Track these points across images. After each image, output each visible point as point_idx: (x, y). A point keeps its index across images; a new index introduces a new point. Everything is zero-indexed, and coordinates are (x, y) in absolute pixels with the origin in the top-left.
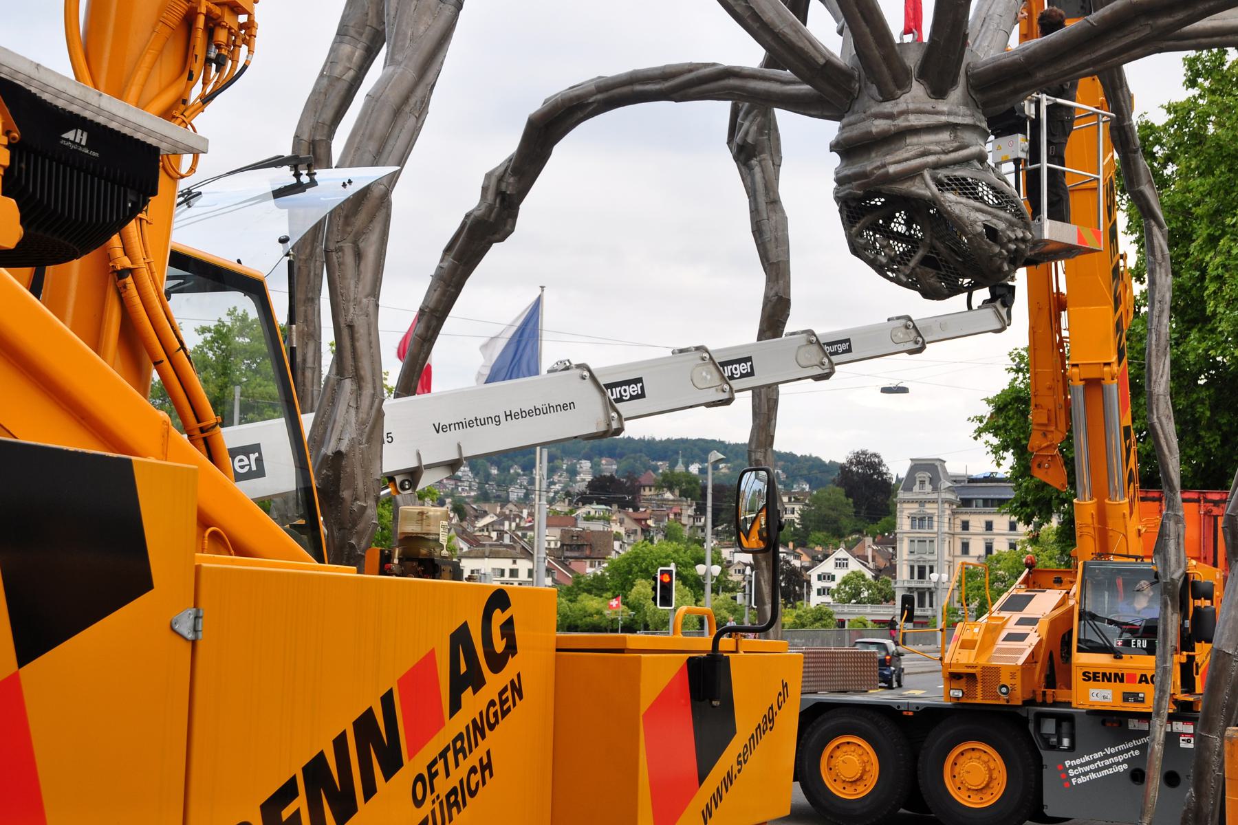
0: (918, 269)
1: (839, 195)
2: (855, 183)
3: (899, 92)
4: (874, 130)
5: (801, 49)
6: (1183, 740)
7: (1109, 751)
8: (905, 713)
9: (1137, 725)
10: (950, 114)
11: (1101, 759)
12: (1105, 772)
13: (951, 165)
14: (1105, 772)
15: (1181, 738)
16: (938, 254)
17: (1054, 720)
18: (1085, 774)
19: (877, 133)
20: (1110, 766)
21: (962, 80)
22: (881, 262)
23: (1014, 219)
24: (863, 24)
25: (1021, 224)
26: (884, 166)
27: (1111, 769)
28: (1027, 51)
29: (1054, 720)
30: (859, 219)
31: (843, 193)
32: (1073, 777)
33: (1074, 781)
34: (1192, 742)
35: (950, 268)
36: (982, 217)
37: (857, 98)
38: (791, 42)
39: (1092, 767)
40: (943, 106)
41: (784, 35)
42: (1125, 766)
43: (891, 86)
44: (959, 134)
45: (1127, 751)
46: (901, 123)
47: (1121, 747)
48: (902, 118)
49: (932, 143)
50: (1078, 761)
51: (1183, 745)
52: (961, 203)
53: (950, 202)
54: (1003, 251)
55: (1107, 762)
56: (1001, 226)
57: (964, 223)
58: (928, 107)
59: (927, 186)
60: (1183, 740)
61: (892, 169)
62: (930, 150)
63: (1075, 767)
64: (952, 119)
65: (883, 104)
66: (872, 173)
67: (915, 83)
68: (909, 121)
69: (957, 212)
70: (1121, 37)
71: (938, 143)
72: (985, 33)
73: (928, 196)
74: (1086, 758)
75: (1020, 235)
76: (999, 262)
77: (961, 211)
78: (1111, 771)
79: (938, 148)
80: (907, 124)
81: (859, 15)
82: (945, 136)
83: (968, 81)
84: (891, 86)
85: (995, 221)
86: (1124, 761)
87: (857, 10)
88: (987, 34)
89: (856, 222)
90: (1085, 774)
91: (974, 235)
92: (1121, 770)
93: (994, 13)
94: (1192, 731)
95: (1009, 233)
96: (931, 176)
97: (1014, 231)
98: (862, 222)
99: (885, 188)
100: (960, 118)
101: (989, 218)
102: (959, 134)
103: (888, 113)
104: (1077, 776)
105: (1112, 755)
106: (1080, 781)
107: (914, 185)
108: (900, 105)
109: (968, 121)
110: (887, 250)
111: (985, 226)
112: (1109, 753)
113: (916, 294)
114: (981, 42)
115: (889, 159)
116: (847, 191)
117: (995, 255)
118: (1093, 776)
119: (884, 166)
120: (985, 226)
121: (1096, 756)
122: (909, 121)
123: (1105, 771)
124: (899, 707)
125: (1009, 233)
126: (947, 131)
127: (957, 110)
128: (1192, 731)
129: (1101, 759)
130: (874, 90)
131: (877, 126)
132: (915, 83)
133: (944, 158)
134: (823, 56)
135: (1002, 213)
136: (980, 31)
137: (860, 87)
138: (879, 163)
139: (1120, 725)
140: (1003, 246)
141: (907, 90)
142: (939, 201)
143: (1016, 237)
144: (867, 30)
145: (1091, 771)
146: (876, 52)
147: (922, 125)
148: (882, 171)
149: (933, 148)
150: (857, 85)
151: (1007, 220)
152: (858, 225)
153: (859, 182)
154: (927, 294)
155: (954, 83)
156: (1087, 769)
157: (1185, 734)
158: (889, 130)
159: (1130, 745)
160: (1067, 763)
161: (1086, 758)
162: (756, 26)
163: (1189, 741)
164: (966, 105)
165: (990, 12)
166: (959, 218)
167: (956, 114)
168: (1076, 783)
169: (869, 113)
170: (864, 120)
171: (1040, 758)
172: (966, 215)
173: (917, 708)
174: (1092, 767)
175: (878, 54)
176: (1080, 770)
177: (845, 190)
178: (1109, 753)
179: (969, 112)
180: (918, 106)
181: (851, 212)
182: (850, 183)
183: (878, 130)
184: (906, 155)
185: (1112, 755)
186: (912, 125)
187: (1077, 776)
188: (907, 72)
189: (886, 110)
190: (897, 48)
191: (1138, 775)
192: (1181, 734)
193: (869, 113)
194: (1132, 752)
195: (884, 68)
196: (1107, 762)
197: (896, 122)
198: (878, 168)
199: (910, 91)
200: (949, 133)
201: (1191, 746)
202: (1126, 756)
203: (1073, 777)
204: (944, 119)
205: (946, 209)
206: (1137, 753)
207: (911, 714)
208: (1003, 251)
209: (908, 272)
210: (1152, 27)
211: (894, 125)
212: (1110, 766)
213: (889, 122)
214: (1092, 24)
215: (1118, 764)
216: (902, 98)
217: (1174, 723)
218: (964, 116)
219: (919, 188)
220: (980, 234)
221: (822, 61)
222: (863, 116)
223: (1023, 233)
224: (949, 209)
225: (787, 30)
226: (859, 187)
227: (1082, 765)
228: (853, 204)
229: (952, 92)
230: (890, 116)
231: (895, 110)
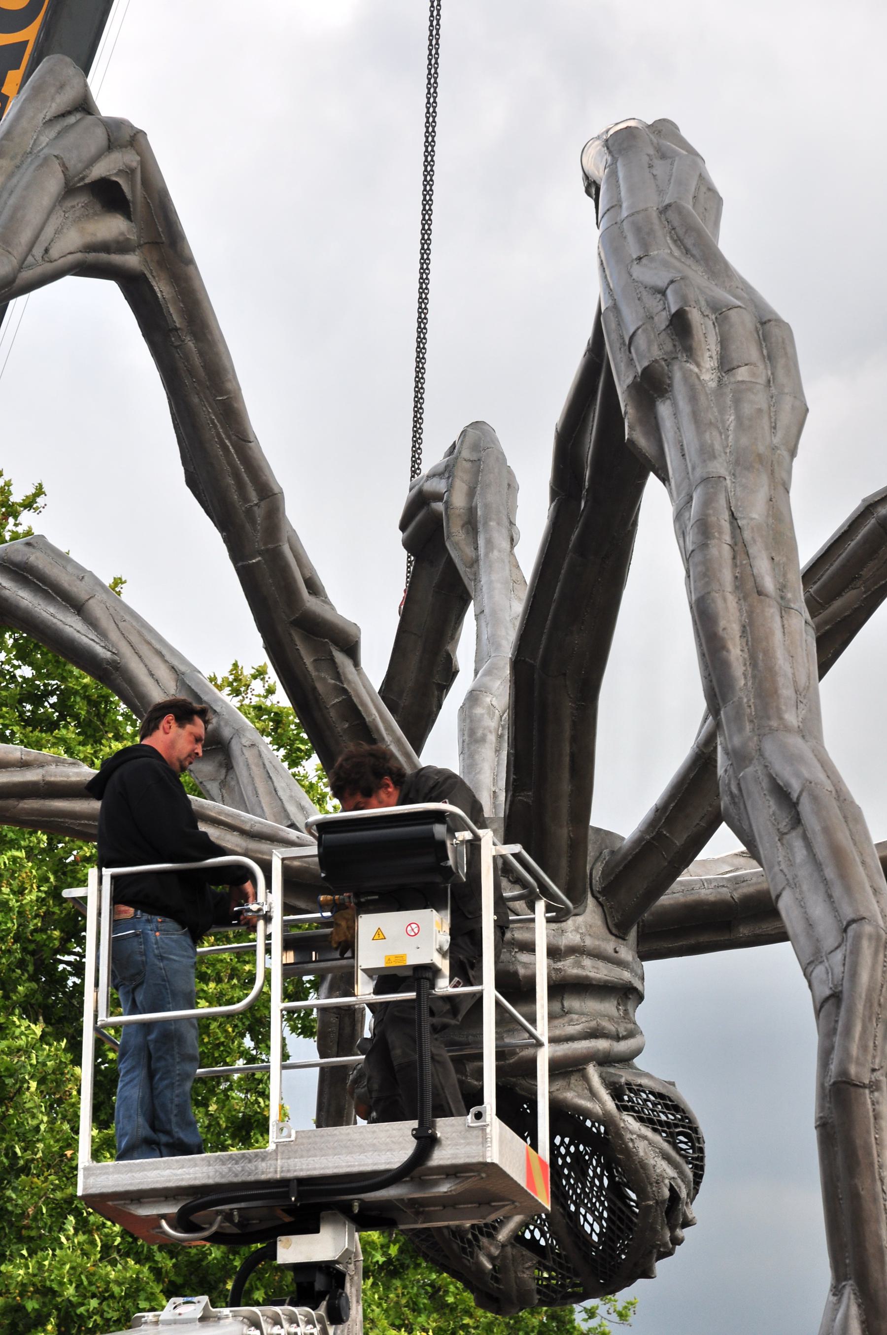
53: (632, 1133)
59: (593, 1095)
68: (583, 967)
69: (641, 1154)
80: (575, 971)
96: (601, 1076)
122: (583, 967)
147: (599, 980)
166: (643, 1165)
175: (565, 836)
180: (597, 943)
186: (587, 978)
199: (584, 911)
200: (615, 1003)
205: (627, 1147)
219: (579, 1096)
224: (631, 1145)
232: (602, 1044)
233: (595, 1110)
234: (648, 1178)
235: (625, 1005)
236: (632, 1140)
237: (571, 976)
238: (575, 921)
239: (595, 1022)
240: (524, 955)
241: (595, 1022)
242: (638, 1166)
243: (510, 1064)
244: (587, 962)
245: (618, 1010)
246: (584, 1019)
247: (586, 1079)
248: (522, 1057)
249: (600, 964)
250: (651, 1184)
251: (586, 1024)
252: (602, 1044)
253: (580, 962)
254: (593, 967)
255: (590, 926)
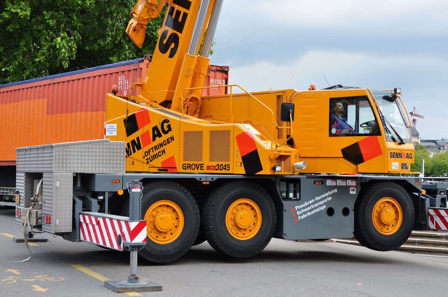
6: (351, 190)
7: (318, 198)
8: (204, 183)
9: (330, 183)
11: (313, 204)
12: (315, 211)
14: (315, 211)
15: (351, 189)
17: (285, 183)
18: (305, 213)
20: (317, 207)
27: (318, 209)
29: (285, 183)
32: (299, 215)
33: (299, 218)
34: (355, 191)
39: (309, 208)
42: (325, 207)
45: (325, 198)
47: (323, 196)
50: (302, 206)
51: (351, 192)
55: (316, 205)
60: (351, 190)
63: (299, 210)
74: (306, 204)
78: (318, 210)
86: (325, 204)
90: (305, 213)
92: (323, 209)
94: (355, 185)
104: (301, 215)
105: (319, 201)
106: (302, 217)
112: (317, 200)
118: (309, 214)
121: (311, 202)
123: (315, 210)
124: (200, 179)
128: (355, 185)
129: (313, 204)
139: (322, 184)
145: (308, 211)
156: (306, 210)
157: (352, 186)
159: (327, 194)
160: (296, 207)
161: (306, 204)
163: (354, 190)
168: (301, 219)
171: (282, 205)
173: (212, 179)
174: (309, 208)
176: (303, 211)
178: (317, 200)
185: (319, 201)
187: (301, 215)
191: (330, 212)
192: (350, 187)
194: (328, 198)
196: (316, 205)
201: (355, 193)
202: (325, 201)
203: (299, 215)
206: (330, 198)
207: (208, 183)
212: (317, 207)
215: (321, 205)
217: (347, 181)
227: (304, 208)
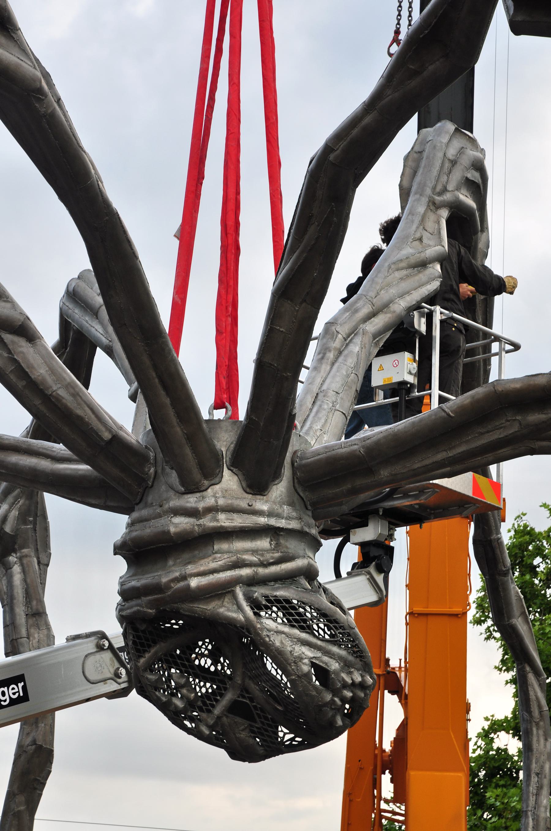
0: (225, 719)
1: (124, 613)
2: (145, 599)
3: (206, 483)
4: (172, 530)
5: (80, 418)
10: (270, 514)
13: (270, 581)
16: (251, 700)
19: (175, 534)
21: (287, 472)
22: (176, 706)
23: (351, 658)
24: (162, 393)
25: (359, 664)
26: (184, 578)
28: (369, 441)
30: (149, 646)
31: (129, 611)
35: (266, 718)
36: (308, 653)
37: (152, 486)
38: (66, 407)
40: (262, 505)
41: (59, 399)
43: (196, 474)
44: (282, 541)
46: (208, 522)
48: (209, 516)
49: (246, 551)
52: (283, 633)
53: (269, 630)
54: (336, 699)
56: (334, 666)
57: (286, 660)
58: (243, 504)
59: (240, 608)
61: (194, 583)
62: (244, 560)
64: (273, 522)
65: (186, 496)
66: (167, 586)
67: (226, 473)
68: (218, 521)
69: (278, 644)
70: (482, 434)
71: (254, 552)
72: (317, 412)
73: (240, 621)
75: (358, 678)
76: (330, 714)
77: (282, 643)
79: (254, 559)
81: (157, 380)
82: (264, 543)
83: (294, 474)
84: (196, 474)
85: (326, 659)
87: (154, 374)
88: (320, 415)
89: (145, 651)
91: (298, 676)
93: (328, 389)
95: (344, 675)
96: (245, 595)
97: (350, 673)
98: (153, 651)
99: (186, 607)
100: (283, 521)
101: (319, 654)
102: (282, 541)
103: (192, 508)
107: (222, 606)
108: (207, 500)
109: (294, 525)
110: (184, 691)
111: (313, 665)
113: (222, 753)
114: (312, 423)
115: (191, 569)
116: (135, 609)
117: (326, 704)
119: (184, 578)
120: (313, 665)
125: (344, 675)
126: (266, 536)
127: (280, 511)
130: (173, 477)
131: (176, 525)
132: (226, 473)
133: (262, 571)
134: (109, 429)
135: (335, 649)
136: (311, 410)
137: (156, 472)
138: (177, 574)
140: (336, 692)
141: (217, 480)
142: (255, 628)
143: (352, 679)
144: (167, 401)
146: (178, 429)
147: (234, 527)
148: (182, 584)
149: (248, 557)
150: (152, 470)
151: (340, 658)
152: (147, 655)
153: (150, 598)
154: (235, 755)
155: (276, 476)
158: (192, 532)
162: (21, 384)
164: (291, 504)
165: (325, 387)
167: (278, 516)
169: (166, 506)
170: (159, 516)
172: (289, 649)
177: (131, 607)
179: (294, 514)
180: (230, 502)
181: (139, 637)
182: (138, 597)
183: (178, 530)
184: (213, 565)
186: (222, 527)
188: (217, 457)
189: (189, 505)
190: (205, 426)
193: (166, 506)
195: (188, 451)
197: (201, 521)
198: (177, 580)
199: (220, 482)
200: (268, 540)
204: (262, 520)
208: (336, 699)
209: (211, 722)
210: (520, 424)
211: (199, 525)
213: (192, 520)
214: (448, 415)
216: (209, 490)
218: (288, 518)
219: (229, 610)
220: (307, 675)
221: (107, 436)
222: (158, 510)
223: (362, 676)
224: (267, 639)
225: (62, 393)
226: (151, 604)
228: (143, 627)
229: (275, 487)
230: (193, 513)
231: (201, 506)
232: (245, 572)
233: (239, 619)
234: (286, 661)
235: (278, 540)
236: (268, 636)
237: (209, 528)
238: (213, 489)
239: (235, 557)
240: (177, 519)
241: (235, 557)
242: (276, 653)
243: (168, 595)
244: (222, 516)
245: (271, 544)
246: (226, 556)
247: (235, 597)
248: (176, 589)
249: (235, 516)
250: (290, 665)
251: (228, 560)
252: (245, 572)
253: (216, 517)
254: (228, 519)
255: (226, 491)
